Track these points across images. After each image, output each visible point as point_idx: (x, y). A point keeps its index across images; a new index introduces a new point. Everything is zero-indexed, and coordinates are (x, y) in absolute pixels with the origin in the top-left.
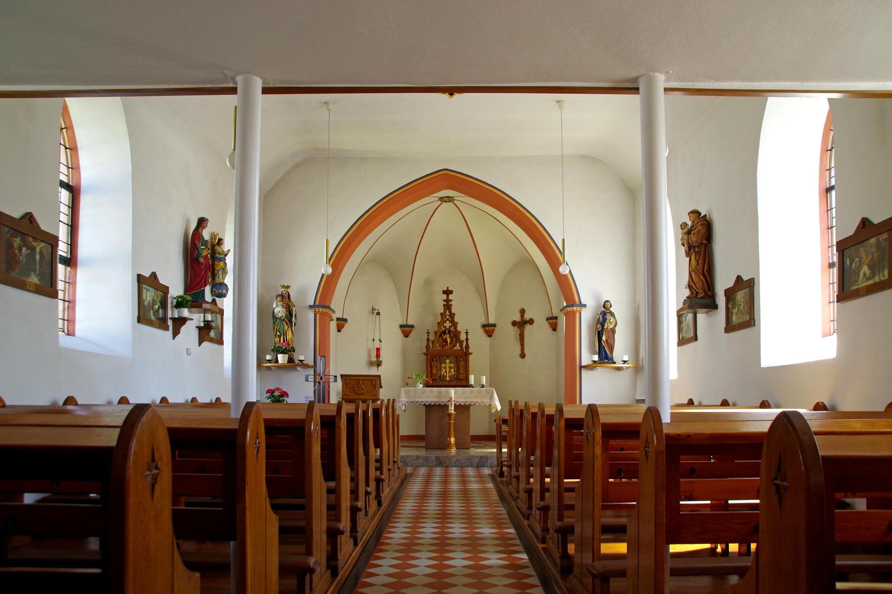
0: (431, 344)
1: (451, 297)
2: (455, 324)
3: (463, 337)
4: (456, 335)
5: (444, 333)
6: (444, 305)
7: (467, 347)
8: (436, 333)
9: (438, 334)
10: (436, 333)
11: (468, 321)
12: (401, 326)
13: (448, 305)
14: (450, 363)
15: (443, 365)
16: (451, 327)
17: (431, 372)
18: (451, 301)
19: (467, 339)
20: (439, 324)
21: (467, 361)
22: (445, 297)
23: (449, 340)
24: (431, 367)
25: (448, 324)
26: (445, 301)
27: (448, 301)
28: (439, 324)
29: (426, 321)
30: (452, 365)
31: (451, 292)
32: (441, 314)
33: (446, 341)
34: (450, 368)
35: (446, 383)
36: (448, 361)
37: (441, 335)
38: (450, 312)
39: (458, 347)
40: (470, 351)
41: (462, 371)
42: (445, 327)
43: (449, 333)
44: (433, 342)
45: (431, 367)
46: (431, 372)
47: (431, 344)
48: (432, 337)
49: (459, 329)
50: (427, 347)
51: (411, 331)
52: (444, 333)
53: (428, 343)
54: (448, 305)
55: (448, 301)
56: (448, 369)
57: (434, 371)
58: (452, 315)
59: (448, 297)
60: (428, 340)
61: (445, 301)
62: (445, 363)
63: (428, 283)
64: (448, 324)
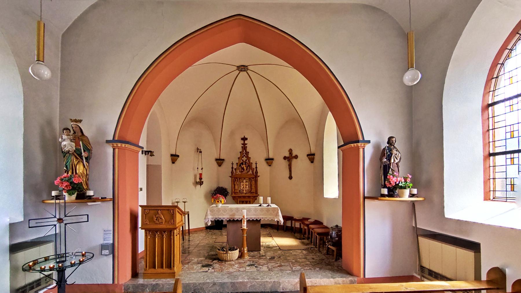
0: (234, 170)
1: (246, 142)
2: (248, 158)
3: (254, 166)
4: (249, 165)
5: (242, 164)
6: (242, 147)
7: (257, 172)
8: (237, 164)
9: (239, 165)
10: (237, 164)
11: (257, 156)
12: (216, 160)
13: (244, 147)
14: (246, 182)
15: (242, 183)
16: (246, 160)
17: (234, 187)
18: (246, 144)
19: (256, 168)
20: (239, 158)
21: (256, 181)
22: (242, 142)
23: (245, 168)
24: (234, 185)
25: (244, 159)
26: (242, 144)
27: (244, 144)
28: (239, 158)
29: (232, 157)
30: (247, 183)
31: (246, 139)
32: (241, 152)
33: (243, 169)
34: (246, 185)
35: (244, 195)
36: (245, 181)
37: (240, 165)
38: (246, 151)
39: (251, 172)
40: (258, 175)
41: (253, 187)
42: (243, 160)
43: (245, 164)
44: (235, 169)
45: (234, 185)
46: (234, 187)
47: (234, 170)
48: (235, 166)
49: (251, 161)
50: (232, 172)
51: (222, 163)
52: (242, 164)
53: (232, 170)
54: (244, 147)
55: (244, 144)
56: (244, 186)
57: (236, 187)
58: (247, 153)
59: (244, 142)
60: (232, 168)
61: (242, 144)
62: (243, 182)
63: (232, 134)
64: (244, 159)
